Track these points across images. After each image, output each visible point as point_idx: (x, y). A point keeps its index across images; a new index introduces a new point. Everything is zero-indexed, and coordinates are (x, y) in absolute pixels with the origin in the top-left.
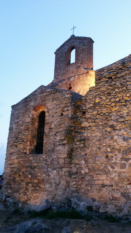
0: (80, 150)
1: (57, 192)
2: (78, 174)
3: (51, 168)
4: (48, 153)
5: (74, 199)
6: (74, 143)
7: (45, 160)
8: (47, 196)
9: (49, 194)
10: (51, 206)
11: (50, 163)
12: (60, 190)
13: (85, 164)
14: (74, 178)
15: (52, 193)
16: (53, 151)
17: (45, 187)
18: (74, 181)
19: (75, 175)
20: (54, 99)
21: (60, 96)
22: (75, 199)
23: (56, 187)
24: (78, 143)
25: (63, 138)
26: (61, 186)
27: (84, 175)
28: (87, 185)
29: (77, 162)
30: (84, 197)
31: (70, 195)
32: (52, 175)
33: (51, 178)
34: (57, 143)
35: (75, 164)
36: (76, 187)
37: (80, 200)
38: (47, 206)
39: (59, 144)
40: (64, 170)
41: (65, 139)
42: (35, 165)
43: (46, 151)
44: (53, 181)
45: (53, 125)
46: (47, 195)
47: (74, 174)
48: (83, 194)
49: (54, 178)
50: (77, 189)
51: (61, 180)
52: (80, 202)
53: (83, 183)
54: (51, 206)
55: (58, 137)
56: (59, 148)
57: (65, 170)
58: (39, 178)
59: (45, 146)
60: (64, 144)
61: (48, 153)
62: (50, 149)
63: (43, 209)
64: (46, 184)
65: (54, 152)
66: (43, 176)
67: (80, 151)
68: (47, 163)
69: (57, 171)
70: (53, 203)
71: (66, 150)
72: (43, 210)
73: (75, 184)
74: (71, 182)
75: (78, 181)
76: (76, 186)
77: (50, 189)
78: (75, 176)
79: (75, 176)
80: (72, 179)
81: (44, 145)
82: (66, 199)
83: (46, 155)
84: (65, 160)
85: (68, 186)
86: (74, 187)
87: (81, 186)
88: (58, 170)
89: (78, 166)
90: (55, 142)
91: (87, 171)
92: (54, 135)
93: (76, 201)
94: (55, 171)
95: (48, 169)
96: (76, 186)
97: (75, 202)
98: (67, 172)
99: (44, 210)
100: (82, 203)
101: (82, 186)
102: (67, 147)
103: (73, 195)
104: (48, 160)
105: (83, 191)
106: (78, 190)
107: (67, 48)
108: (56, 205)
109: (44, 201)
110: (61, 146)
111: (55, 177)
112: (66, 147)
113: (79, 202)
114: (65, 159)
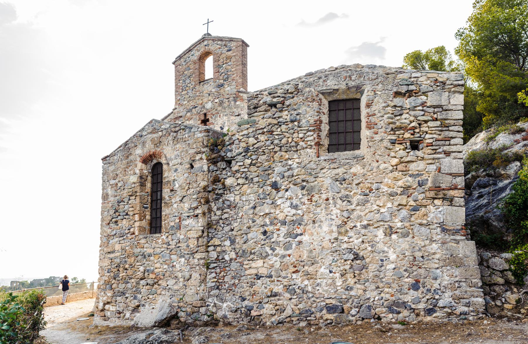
1: (187, 291)
2: (220, 262)
4: (170, 231)
5: (213, 300)
7: (166, 244)
8: (171, 298)
9: (174, 294)
10: (177, 313)
11: (174, 246)
12: (192, 288)
13: (230, 246)
14: (214, 268)
15: (179, 293)
18: (212, 272)
19: (214, 263)
22: (215, 299)
23: (185, 283)
24: (219, 213)
26: (192, 281)
27: (229, 262)
28: (234, 278)
29: (217, 242)
30: (228, 295)
31: (207, 294)
33: (177, 270)
36: (216, 281)
37: (222, 300)
38: (171, 312)
42: (149, 251)
43: (166, 229)
44: (180, 275)
46: (170, 297)
47: (213, 262)
48: (227, 290)
50: (218, 284)
51: (192, 272)
52: (223, 303)
53: (226, 275)
54: (177, 313)
58: (156, 271)
59: (165, 220)
61: (170, 231)
62: (172, 224)
63: (165, 317)
64: (168, 280)
65: (180, 229)
66: (164, 268)
67: (222, 225)
68: (169, 247)
70: (180, 308)
71: (200, 225)
72: (165, 319)
73: (215, 278)
74: (208, 274)
75: (220, 273)
76: (216, 280)
77: (176, 287)
78: (215, 265)
79: (215, 265)
80: (210, 270)
81: (163, 218)
82: (200, 300)
83: (167, 234)
84: (198, 241)
85: (203, 280)
86: (213, 282)
87: (224, 279)
89: (219, 249)
93: (216, 302)
95: (172, 256)
96: (216, 280)
97: (215, 303)
99: (166, 318)
100: (225, 305)
101: (226, 279)
103: (211, 293)
105: (226, 287)
106: (219, 286)
108: (184, 309)
109: (167, 305)
111: (183, 268)
113: (220, 303)
114: (198, 240)
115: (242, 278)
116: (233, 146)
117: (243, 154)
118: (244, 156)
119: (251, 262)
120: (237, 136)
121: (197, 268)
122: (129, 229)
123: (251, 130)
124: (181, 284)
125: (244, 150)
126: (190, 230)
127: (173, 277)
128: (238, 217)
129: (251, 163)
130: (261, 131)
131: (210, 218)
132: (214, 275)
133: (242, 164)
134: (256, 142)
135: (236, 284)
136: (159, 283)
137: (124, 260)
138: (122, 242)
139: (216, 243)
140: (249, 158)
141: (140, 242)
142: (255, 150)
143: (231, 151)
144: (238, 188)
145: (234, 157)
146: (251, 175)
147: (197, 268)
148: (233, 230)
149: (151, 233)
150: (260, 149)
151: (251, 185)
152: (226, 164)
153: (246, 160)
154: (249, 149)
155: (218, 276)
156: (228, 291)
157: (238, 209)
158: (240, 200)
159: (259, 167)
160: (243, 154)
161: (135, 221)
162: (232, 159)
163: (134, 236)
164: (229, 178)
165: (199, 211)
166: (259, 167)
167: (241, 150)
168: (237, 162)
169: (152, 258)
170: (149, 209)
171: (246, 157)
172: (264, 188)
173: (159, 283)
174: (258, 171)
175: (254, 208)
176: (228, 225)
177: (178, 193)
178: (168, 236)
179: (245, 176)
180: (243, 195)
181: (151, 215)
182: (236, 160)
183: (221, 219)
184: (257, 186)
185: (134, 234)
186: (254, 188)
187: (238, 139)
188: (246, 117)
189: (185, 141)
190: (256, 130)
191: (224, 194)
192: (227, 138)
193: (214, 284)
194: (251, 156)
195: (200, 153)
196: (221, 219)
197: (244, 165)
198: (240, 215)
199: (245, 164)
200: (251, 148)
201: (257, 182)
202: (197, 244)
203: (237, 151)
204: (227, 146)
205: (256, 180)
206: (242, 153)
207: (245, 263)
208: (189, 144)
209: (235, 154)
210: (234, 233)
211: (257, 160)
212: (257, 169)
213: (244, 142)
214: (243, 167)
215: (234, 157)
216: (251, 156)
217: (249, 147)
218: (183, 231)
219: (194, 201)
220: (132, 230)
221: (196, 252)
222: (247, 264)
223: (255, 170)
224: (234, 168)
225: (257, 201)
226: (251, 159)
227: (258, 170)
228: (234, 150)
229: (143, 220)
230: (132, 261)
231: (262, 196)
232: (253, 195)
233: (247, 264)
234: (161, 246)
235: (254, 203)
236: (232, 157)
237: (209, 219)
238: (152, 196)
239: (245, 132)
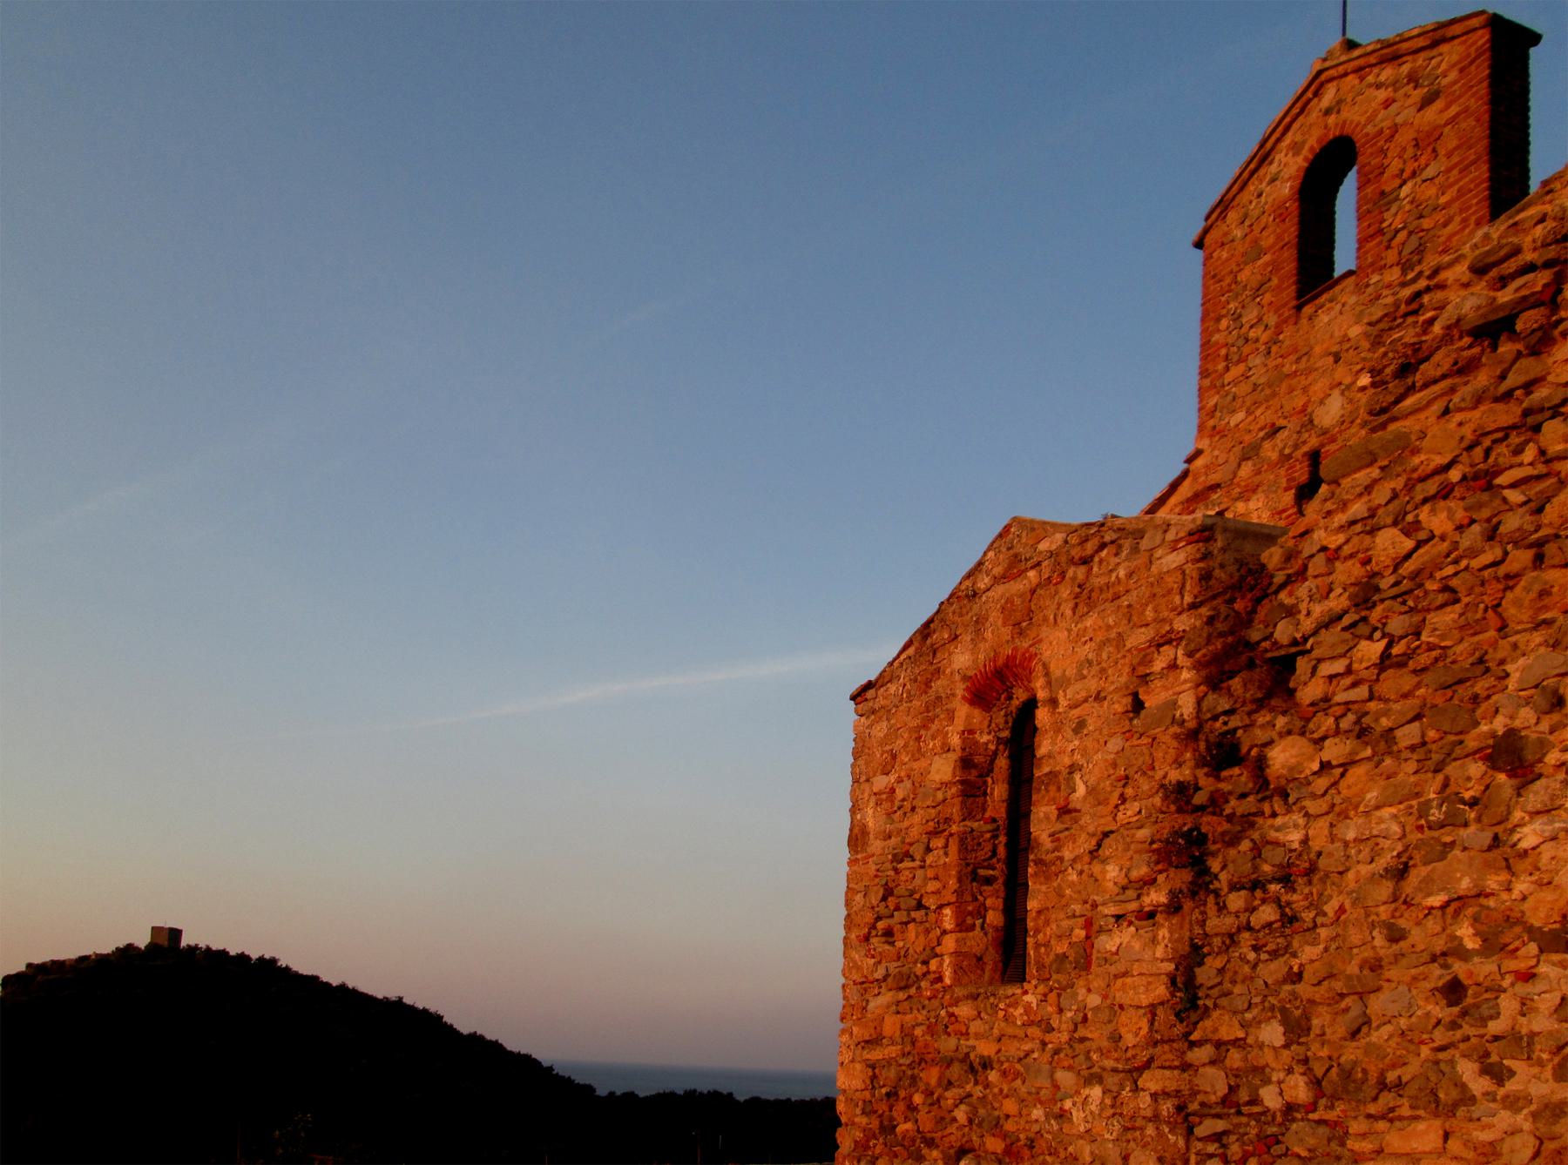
0: (1256, 948)
6: (1211, 900)
21: (1122, 573)
34: (1106, 912)
39: (1118, 917)
41: (1155, 880)
55: (1109, 868)
56: (1118, 941)
60: (1151, 915)
67: (1252, 956)
90: (1095, 906)
92: (1087, 859)
102: (1167, 935)
107: (1295, 168)
110: (1129, 926)
112: (1163, 933)
116: (1302, 590)
117: (1346, 621)
118: (1354, 625)
120: (1320, 536)
125: (1350, 598)
128: (1319, 920)
129: (1385, 655)
131: (1203, 923)
133: (1338, 666)
140: (1377, 635)
143: (1291, 612)
145: (1305, 639)
146: (1386, 713)
150: (1431, 576)
151: (1388, 761)
153: (1364, 644)
154: (1377, 590)
159: (1424, 670)
160: (1346, 621)
162: (1293, 650)
166: (1424, 670)
167: (1338, 601)
168: (1319, 661)
172: (1450, 769)
174: (1422, 691)
175: (1400, 872)
176: (1275, 954)
182: (1316, 653)
183: (1249, 928)
184: (1411, 767)
186: (1401, 776)
187: (1324, 549)
189: (1117, 597)
192: (1272, 557)
195: (1169, 642)
196: (1249, 928)
197: (1349, 671)
199: (1355, 666)
200: (1384, 584)
201: (1412, 748)
203: (1318, 609)
204: (1277, 592)
205: (1408, 735)
206: (1346, 612)
208: (1129, 606)
209: (1307, 625)
211: (1417, 634)
212: (1416, 679)
215: (1305, 639)
217: (1376, 580)
223: (1407, 688)
224: (1309, 692)
225: (1414, 837)
226: (1383, 637)
227: (1418, 686)
228: (1303, 607)
231: (1436, 815)
232: (1393, 810)
235: (1400, 847)
236: (1295, 643)
237: (1198, 930)
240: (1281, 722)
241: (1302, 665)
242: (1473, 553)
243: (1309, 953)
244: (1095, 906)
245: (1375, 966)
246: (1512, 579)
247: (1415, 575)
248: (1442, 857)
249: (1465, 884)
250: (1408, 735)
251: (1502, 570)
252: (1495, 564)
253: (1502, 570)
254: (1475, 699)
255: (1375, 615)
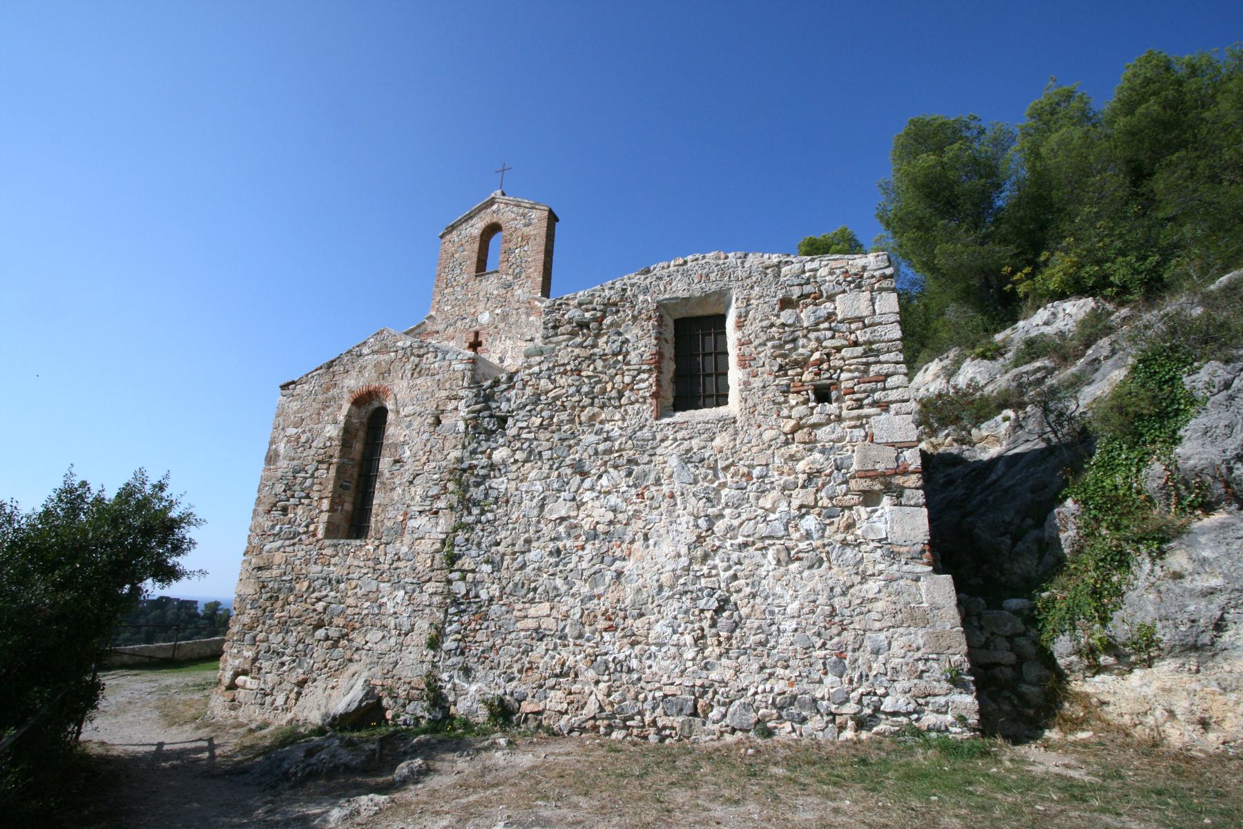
3: (389, 581)
13: (492, 573)
16: (400, 531)
17: (367, 642)
20: (417, 371)
25: (434, 491)
32: (390, 605)
35: (462, 571)
39: (420, 512)
40: (430, 587)
43: (377, 531)
45: (408, 453)
48: (479, 659)
49: (395, 613)
52: (468, 682)
57: (430, 591)
59: (377, 515)
60: (436, 513)
62: (389, 524)
65: (402, 535)
67: (481, 534)
69: (406, 593)
71: (439, 529)
81: (374, 511)
84: (432, 561)
87: (474, 637)
88: (409, 588)
90: (408, 506)
91: (495, 590)
94: (402, 593)
95: (382, 585)
96: (459, 637)
98: (435, 593)
104: (381, 560)
111: (400, 609)
115: (509, 637)
117: (528, 408)
118: (530, 411)
119: (527, 605)
120: (521, 374)
121: (427, 611)
122: (307, 526)
123: (544, 366)
124: (393, 641)
126: (423, 538)
127: (379, 625)
129: (541, 424)
130: (562, 369)
132: (455, 626)
133: (524, 424)
134: (552, 386)
135: (498, 647)
136: (350, 637)
137: (288, 585)
138: (291, 549)
139: (466, 567)
141: (324, 552)
142: (550, 400)
143: (509, 400)
144: (514, 468)
145: (513, 411)
146: (540, 445)
147: (427, 611)
148: (498, 544)
149: (348, 538)
152: (499, 424)
153: (533, 418)
155: (465, 629)
156: (481, 660)
157: (512, 506)
158: (517, 489)
160: (528, 408)
161: (322, 511)
163: (315, 539)
164: (501, 449)
165: (441, 504)
168: (517, 421)
169: (342, 586)
170: (351, 491)
171: (534, 412)
173: (350, 637)
177: (407, 467)
178: (378, 546)
179: (529, 446)
180: (522, 481)
181: (354, 504)
185: (314, 535)
188: (539, 342)
190: (554, 367)
191: (489, 475)
193: (454, 645)
194: (542, 410)
197: (528, 427)
198: (514, 517)
201: (549, 460)
202: (431, 566)
207: (517, 606)
209: (513, 406)
210: (501, 549)
213: (533, 385)
214: (526, 430)
215: (513, 411)
216: (542, 410)
218: (407, 538)
219: (435, 484)
220: (312, 528)
221: (430, 580)
222: (520, 610)
224: (512, 432)
229: (337, 510)
230: (304, 589)
233: (520, 610)
234: (362, 564)
236: (509, 412)
238: (361, 468)
239: (536, 369)
240: (501, 441)
241: (510, 421)
242: (572, 395)
243: (503, 534)
244: (408, 506)
245: (528, 541)
246: (584, 407)
247: (553, 398)
248: (556, 501)
249: (563, 513)
250: (546, 455)
251: (581, 404)
252: (580, 401)
253: (581, 404)
254: (570, 447)
255: (538, 409)
